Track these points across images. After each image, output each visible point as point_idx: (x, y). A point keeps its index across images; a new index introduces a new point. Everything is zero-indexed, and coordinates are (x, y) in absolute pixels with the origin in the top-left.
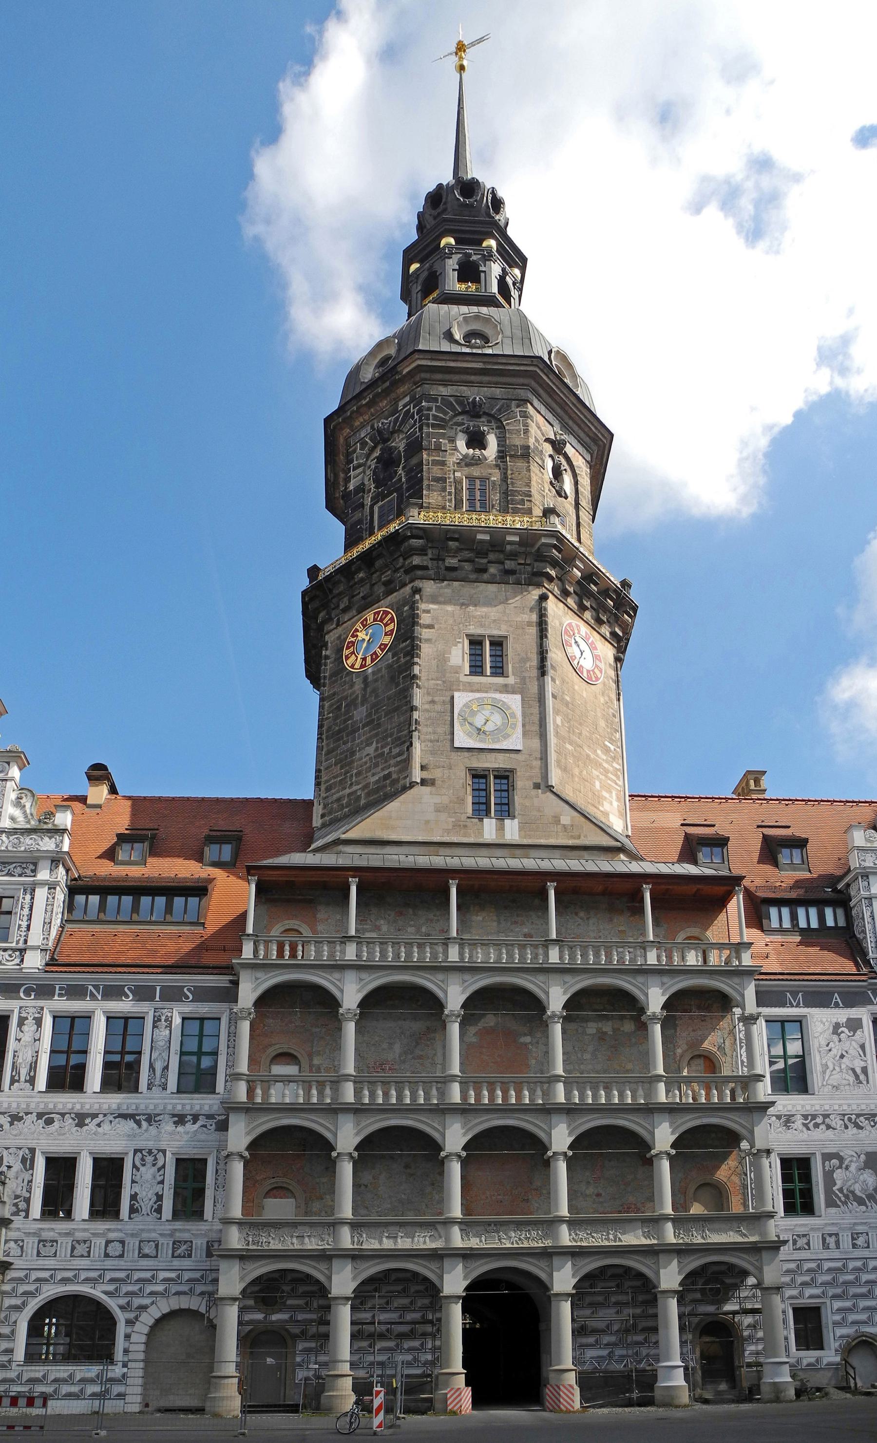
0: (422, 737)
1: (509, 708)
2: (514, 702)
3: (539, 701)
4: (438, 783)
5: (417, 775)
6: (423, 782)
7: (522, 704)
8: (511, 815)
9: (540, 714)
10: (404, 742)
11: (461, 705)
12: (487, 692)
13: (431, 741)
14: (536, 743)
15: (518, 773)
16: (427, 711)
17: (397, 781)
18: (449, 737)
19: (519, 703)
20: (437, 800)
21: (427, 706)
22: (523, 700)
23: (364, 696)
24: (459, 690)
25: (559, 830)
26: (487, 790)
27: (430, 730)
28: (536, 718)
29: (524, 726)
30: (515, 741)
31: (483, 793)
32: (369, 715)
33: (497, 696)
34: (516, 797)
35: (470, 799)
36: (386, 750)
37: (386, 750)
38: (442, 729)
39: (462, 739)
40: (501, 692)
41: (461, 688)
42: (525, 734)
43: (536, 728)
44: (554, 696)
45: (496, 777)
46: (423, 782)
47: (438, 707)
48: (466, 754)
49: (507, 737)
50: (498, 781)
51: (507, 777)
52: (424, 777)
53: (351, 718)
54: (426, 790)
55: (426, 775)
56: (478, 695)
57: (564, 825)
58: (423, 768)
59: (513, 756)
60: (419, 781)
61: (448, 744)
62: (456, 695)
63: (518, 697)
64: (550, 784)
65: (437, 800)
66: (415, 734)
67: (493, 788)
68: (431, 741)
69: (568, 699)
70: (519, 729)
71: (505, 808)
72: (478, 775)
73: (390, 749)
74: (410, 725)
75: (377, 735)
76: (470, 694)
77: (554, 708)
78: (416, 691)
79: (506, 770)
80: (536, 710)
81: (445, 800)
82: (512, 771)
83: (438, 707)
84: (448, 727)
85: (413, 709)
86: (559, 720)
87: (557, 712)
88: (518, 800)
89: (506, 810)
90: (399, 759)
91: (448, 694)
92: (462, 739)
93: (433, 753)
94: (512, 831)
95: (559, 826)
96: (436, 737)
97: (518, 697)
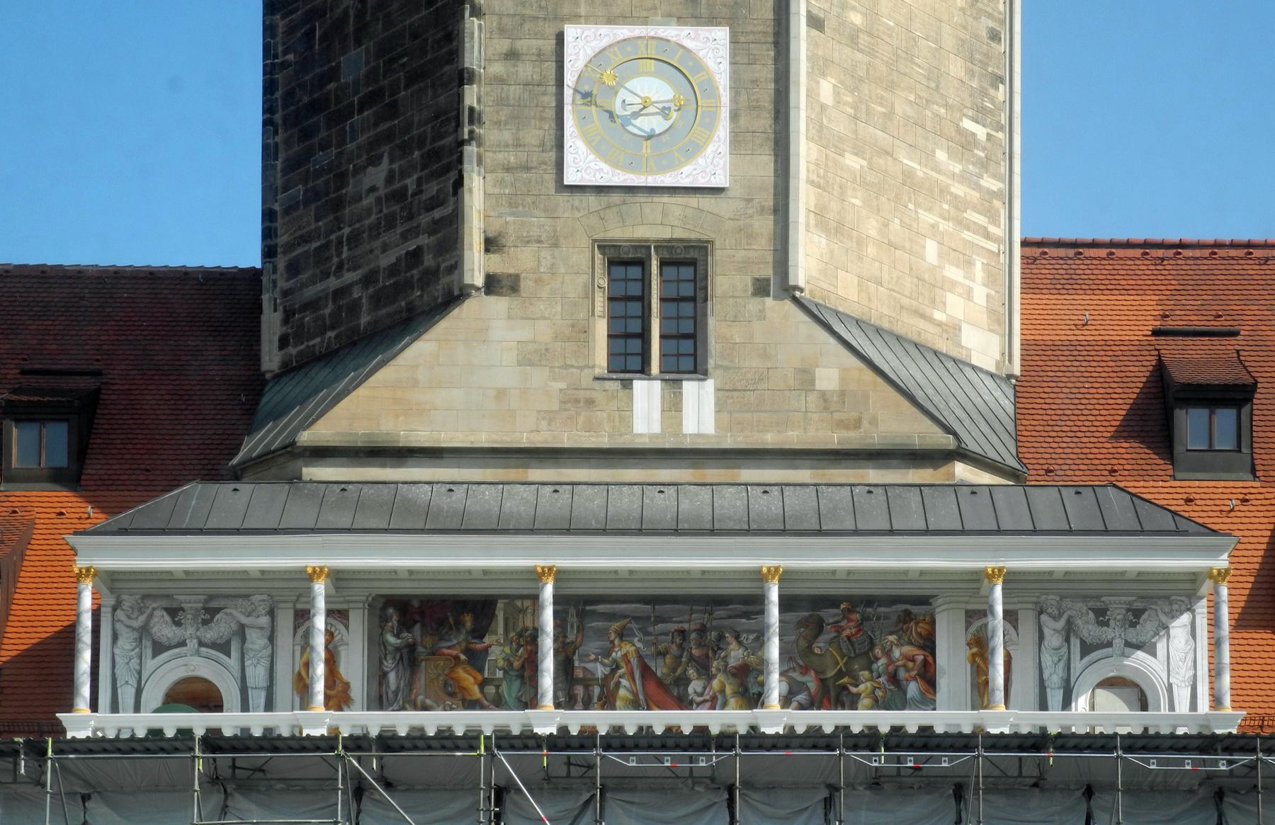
0: (489, 157)
1: (699, 67)
2: (711, 46)
3: (776, 44)
4: (526, 285)
5: (476, 265)
6: (493, 284)
7: (733, 54)
8: (698, 369)
9: (777, 81)
10: (447, 169)
11: (580, 65)
12: (645, 21)
13: (508, 169)
14: (764, 165)
15: (718, 253)
16: (500, 80)
17: (431, 276)
18: (552, 155)
19: (725, 51)
20: (524, 332)
21: (497, 68)
22: (734, 41)
23: (360, 15)
24: (575, 18)
25: (812, 407)
26: (644, 299)
27: (507, 136)
28: (766, 95)
29: (734, 116)
30: (712, 164)
31: (635, 308)
32: (372, 76)
33: (672, 32)
34: (711, 321)
35: (601, 329)
36: (411, 182)
37: (411, 182)
38: (535, 134)
39: (584, 164)
40: (681, 20)
41: (583, 10)
42: (737, 140)
43: (765, 122)
44: (816, 23)
45: (663, 264)
46: (493, 284)
47: (526, 70)
48: (592, 199)
49: (692, 151)
50: (671, 272)
51: (693, 263)
52: (491, 271)
53: (333, 74)
54: (498, 304)
55: (497, 264)
56: (624, 32)
57: (823, 395)
58: (491, 244)
59: (706, 202)
60: (479, 281)
61: (550, 178)
62: (570, 31)
63: (722, 34)
64: (791, 283)
65: (524, 332)
66: (470, 150)
67: (659, 299)
68: (508, 169)
69: (856, 19)
70: (723, 130)
71: (687, 346)
72: (625, 262)
73: (419, 181)
74: (459, 125)
75: (388, 136)
76: (604, 29)
77: (812, 58)
78: (472, 25)
79: (688, 245)
80: (766, 72)
81: (544, 332)
82: (703, 247)
83: (526, 70)
84: (549, 126)
85: (463, 77)
86: (826, 89)
87: (820, 67)
88: (719, 329)
89: (688, 356)
90: (437, 214)
91: (551, 30)
92: (584, 164)
93: (513, 202)
94: (700, 412)
95: (812, 397)
96: (523, 157)
97: (722, 34)
